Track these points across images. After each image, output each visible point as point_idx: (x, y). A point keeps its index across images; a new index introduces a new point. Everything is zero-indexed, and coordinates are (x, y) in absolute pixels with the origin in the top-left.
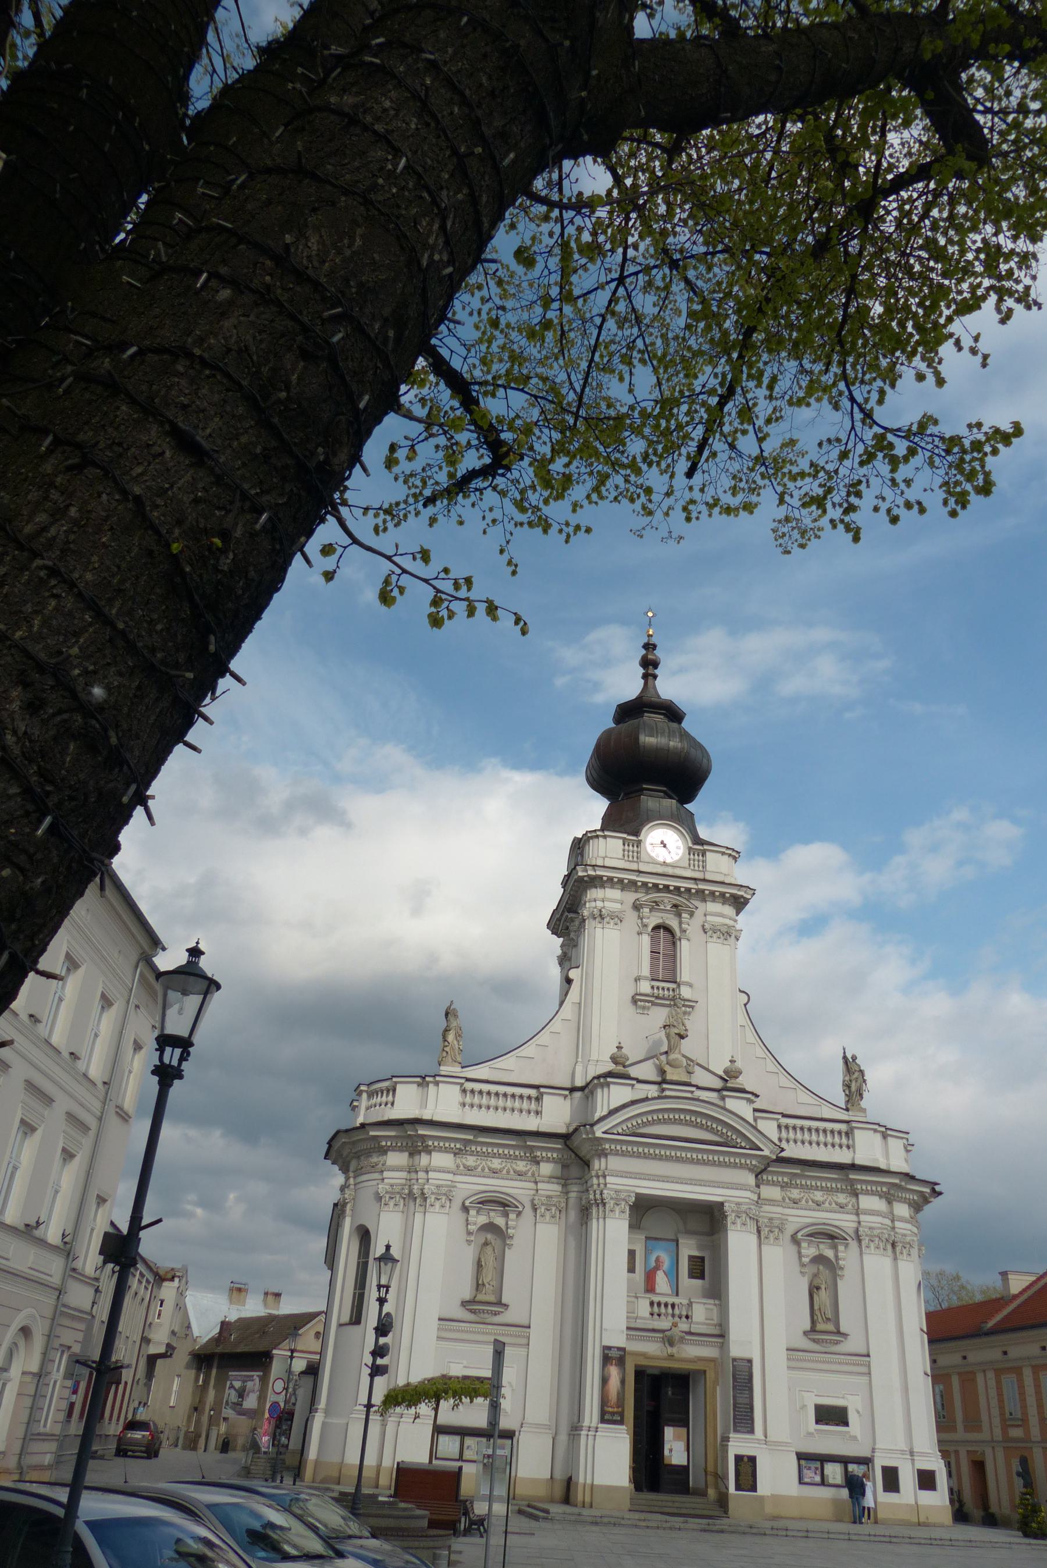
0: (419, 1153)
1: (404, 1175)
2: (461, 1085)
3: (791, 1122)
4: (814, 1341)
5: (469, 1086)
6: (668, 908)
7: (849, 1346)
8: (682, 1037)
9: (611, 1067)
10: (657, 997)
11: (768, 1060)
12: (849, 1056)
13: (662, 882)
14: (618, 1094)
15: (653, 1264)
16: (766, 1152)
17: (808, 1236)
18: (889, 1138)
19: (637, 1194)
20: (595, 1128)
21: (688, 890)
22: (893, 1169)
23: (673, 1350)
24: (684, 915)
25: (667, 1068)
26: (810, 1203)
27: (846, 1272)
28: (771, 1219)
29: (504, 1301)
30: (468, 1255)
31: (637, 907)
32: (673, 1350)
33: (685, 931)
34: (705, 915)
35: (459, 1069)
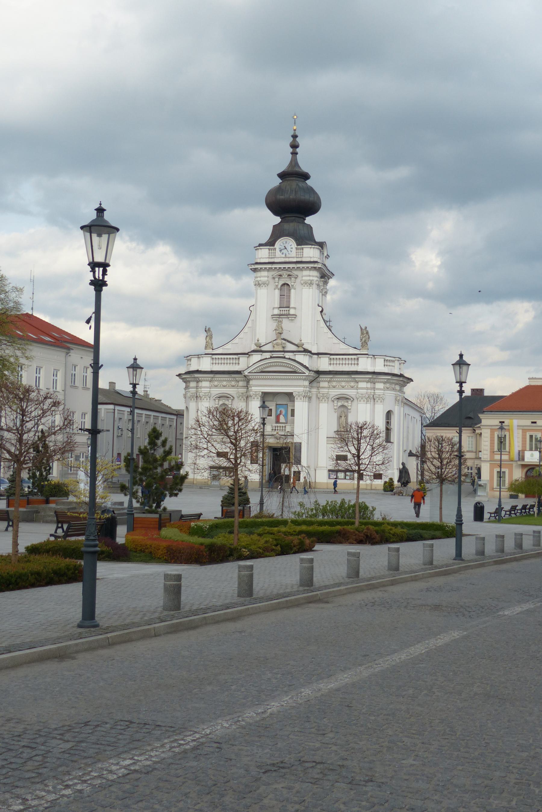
0: (199, 382)
1: (195, 390)
2: (211, 357)
3: (335, 357)
5: (214, 357)
6: (286, 277)
8: (281, 334)
9: (254, 347)
10: (282, 315)
12: (363, 328)
14: (256, 357)
15: (279, 413)
16: (307, 374)
17: (337, 399)
18: (376, 359)
19: (262, 392)
20: (244, 372)
21: (293, 268)
22: (376, 371)
24: (292, 279)
25: (275, 346)
26: (340, 387)
27: (352, 410)
28: (323, 394)
31: (274, 278)
32: (279, 441)
33: (293, 286)
35: (211, 350)
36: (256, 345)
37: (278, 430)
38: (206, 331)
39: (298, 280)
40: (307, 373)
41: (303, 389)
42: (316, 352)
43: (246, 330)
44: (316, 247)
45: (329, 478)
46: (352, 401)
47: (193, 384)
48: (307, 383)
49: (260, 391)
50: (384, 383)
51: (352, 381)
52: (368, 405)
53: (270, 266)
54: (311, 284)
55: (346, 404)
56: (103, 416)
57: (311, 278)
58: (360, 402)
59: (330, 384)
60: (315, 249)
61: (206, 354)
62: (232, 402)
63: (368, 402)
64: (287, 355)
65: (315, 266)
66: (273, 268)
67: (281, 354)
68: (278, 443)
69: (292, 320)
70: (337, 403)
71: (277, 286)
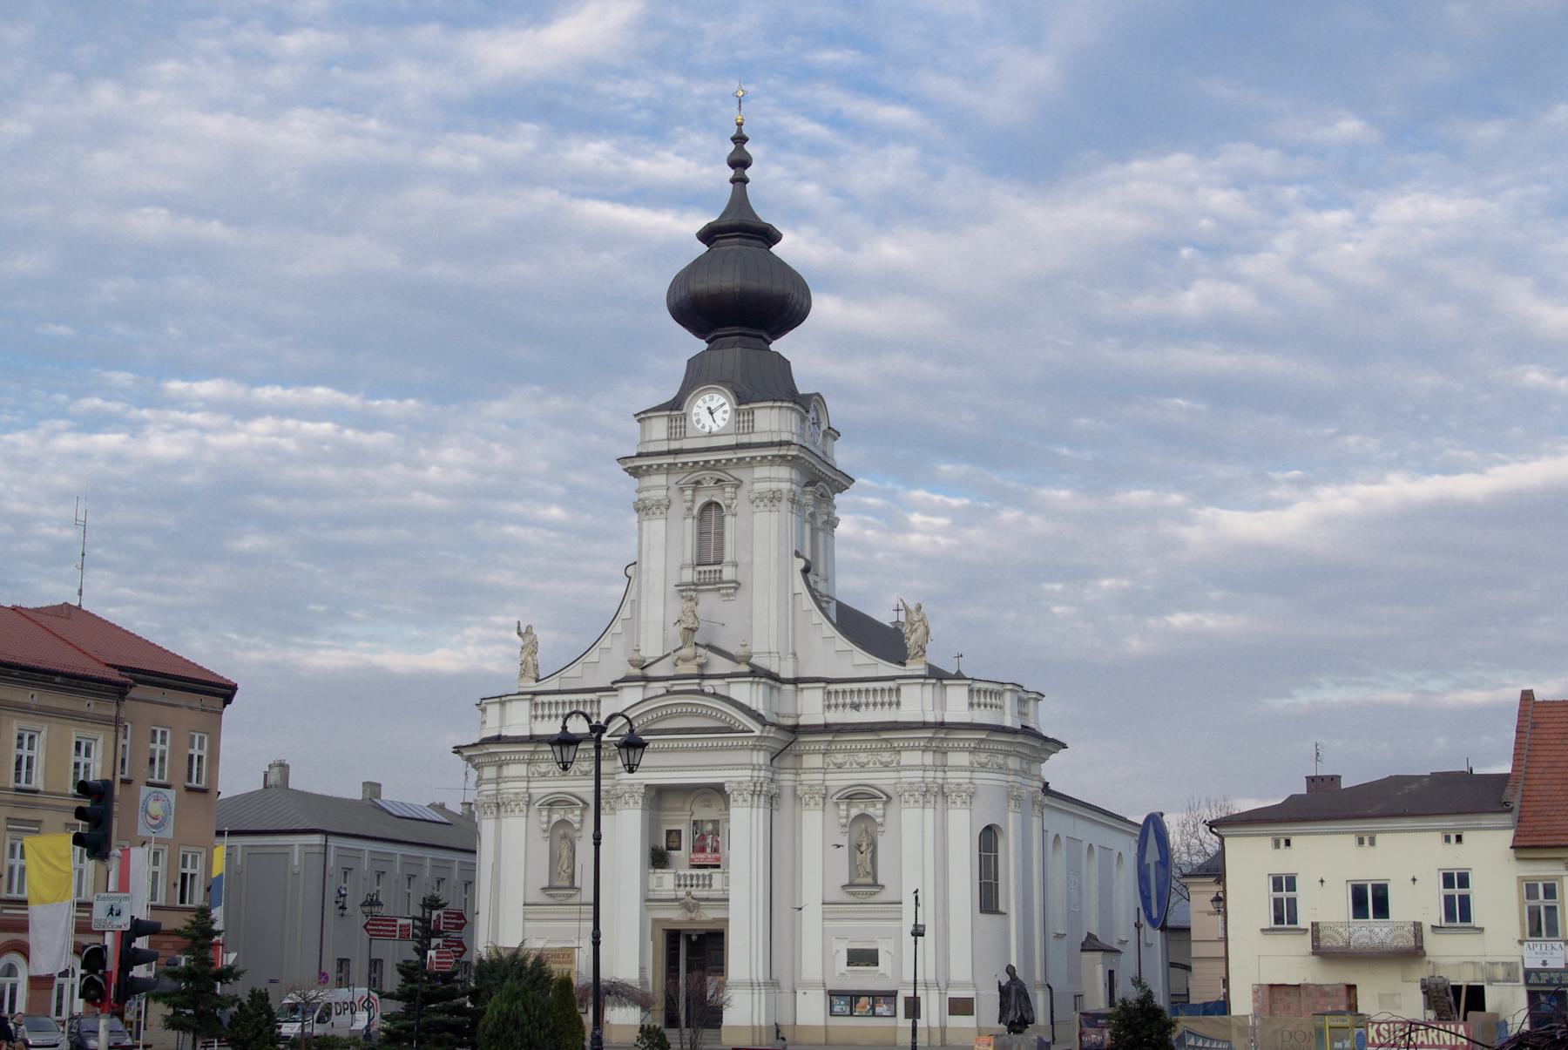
1: (493, 786)
3: (840, 687)
4: (853, 894)
5: (539, 699)
6: (712, 485)
7: (883, 896)
11: (824, 626)
13: (701, 458)
14: (631, 696)
16: (757, 733)
17: (847, 798)
18: (948, 688)
19: (647, 786)
21: (729, 460)
22: (948, 719)
23: (694, 915)
28: (811, 786)
30: (542, 850)
31: (682, 490)
32: (694, 915)
34: (753, 483)
35: (534, 684)
36: (632, 663)
37: (686, 886)
38: (519, 634)
39: (742, 493)
40: (757, 730)
41: (749, 772)
42: (790, 676)
43: (617, 627)
44: (785, 404)
45: (832, 1013)
46: (886, 803)
47: (489, 772)
48: (760, 758)
49: (641, 784)
50: (973, 751)
51: (886, 750)
52: (929, 812)
53: (670, 460)
54: (774, 498)
55: (871, 811)
56: (296, 863)
57: (774, 486)
58: (907, 805)
59: (827, 760)
60: (784, 411)
61: (519, 694)
62: (582, 815)
63: (928, 805)
64: (708, 686)
65: (781, 453)
66: (680, 465)
67: (692, 685)
68: (692, 920)
69: (728, 595)
70: (848, 810)
71: (690, 509)
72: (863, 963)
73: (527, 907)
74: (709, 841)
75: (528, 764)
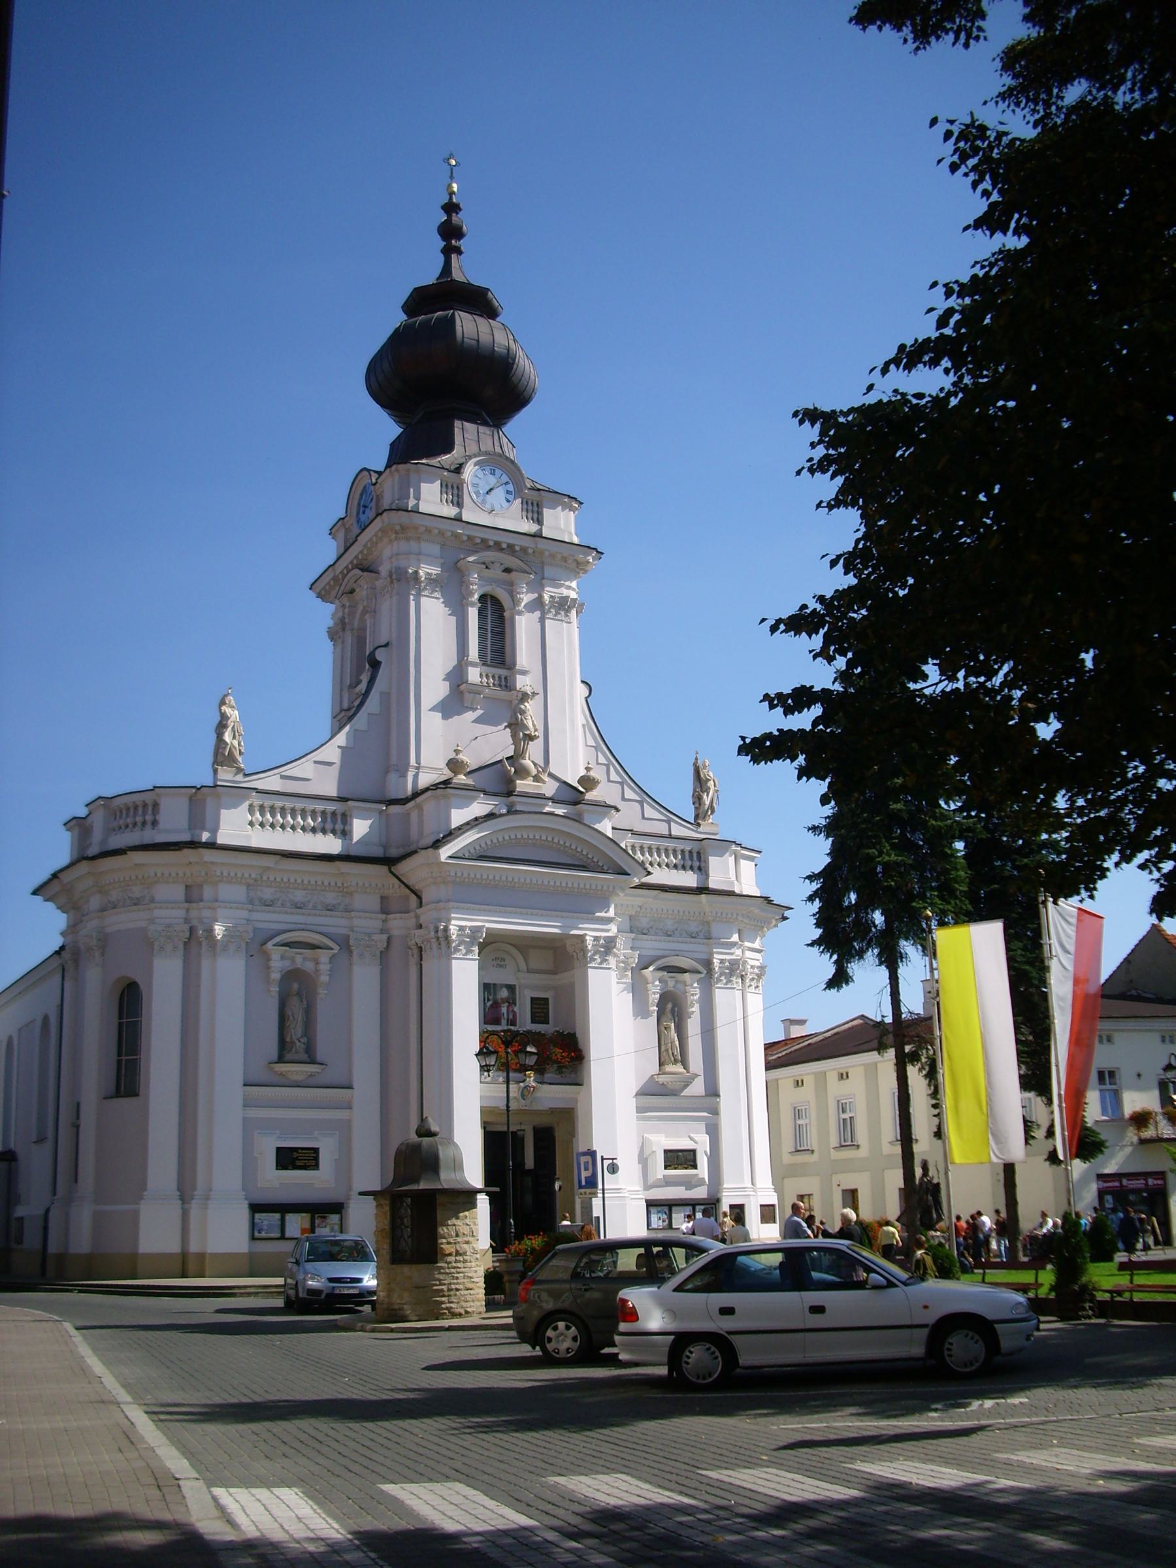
29: (319, 1059)
72: (680, 1167)
73: (248, 1088)
74: (504, 1010)
75: (248, 885)
